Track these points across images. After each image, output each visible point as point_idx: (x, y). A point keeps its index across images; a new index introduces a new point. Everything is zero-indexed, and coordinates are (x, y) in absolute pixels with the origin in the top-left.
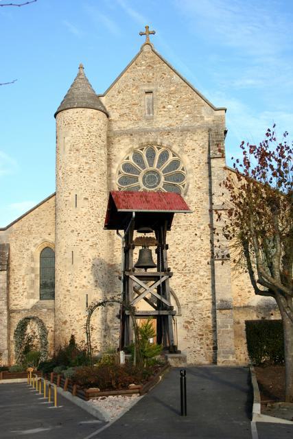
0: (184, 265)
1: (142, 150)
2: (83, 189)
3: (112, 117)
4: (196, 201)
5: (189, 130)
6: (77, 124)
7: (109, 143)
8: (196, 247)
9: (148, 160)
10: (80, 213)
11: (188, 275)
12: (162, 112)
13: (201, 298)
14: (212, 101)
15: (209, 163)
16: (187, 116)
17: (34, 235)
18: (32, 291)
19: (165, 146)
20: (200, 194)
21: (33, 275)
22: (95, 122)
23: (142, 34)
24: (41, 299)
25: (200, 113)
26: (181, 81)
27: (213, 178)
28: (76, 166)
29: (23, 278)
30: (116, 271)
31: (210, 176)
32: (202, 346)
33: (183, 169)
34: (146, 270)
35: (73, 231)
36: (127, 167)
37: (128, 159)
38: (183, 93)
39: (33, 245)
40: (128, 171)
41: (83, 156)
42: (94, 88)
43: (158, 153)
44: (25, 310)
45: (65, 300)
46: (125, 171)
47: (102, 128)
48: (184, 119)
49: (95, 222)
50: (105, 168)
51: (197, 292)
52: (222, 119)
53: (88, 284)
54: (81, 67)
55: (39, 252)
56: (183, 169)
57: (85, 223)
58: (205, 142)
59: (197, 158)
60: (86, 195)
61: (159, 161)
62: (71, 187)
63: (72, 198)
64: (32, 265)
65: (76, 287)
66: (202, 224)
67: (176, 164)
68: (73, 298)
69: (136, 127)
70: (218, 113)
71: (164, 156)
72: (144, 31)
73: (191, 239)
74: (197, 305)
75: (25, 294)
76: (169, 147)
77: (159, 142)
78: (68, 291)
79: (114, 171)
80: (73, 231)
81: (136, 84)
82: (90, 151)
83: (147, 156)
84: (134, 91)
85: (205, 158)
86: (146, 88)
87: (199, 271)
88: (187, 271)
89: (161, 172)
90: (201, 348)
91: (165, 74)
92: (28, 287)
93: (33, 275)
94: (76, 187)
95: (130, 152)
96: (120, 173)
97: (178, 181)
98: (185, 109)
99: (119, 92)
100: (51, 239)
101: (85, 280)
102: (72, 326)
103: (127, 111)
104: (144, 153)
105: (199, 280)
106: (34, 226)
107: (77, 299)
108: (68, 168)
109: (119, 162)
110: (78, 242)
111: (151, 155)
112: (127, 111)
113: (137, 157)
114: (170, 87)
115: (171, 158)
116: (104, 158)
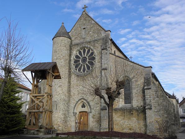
5: (96, 40)
7: (71, 49)
14: (105, 28)
33: (95, 55)
36: (77, 57)
37: (77, 54)
40: (77, 58)
41: (58, 54)
50: (67, 57)
52: (109, 35)
54: (63, 23)
61: (84, 54)
67: (92, 53)
70: (107, 32)
71: (89, 51)
72: (84, 7)
74: (97, 108)
76: (90, 48)
77: (86, 46)
79: (72, 58)
86: (83, 27)
97: (93, 60)
111: (84, 52)
113: (80, 53)
115: (91, 51)
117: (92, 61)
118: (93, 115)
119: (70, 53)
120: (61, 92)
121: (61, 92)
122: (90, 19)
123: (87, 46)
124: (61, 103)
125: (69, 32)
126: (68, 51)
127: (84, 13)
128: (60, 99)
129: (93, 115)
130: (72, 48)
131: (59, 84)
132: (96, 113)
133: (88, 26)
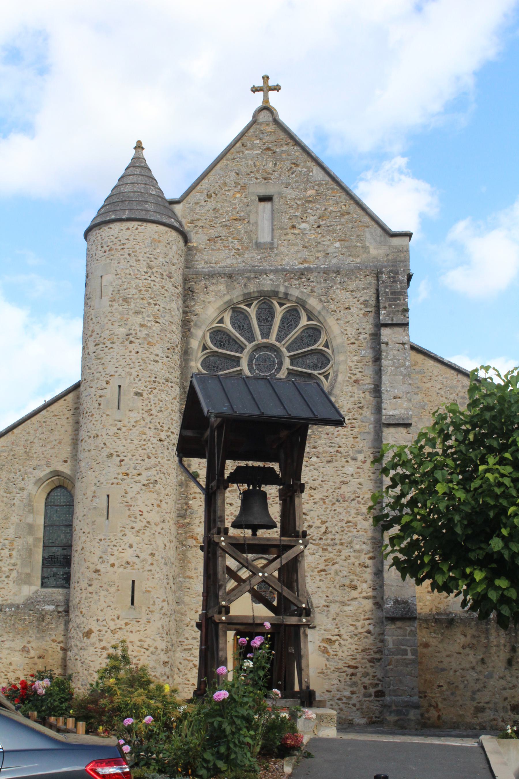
0: (323, 529)
1: (249, 306)
2: (135, 374)
3: (193, 244)
4: (350, 406)
5: (338, 272)
6: (126, 251)
8: (347, 495)
9: (259, 325)
10: (126, 422)
11: (330, 549)
12: (290, 237)
13: (354, 594)
15: (376, 336)
16: (337, 244)
17: (34, 463)
18: (28, 570)
19: (294, 299)
20: (358, 395)
21: (30, 540)
22: (161, 249)
23: (255, 90)
24: (44, 585)
25: (361, 241)
26: (327, 178)
27: (384, 362)
28: (123, 331)
29: (11, 543)
30: (192, 537)
31: (377, 359)
32: (355, 689)
33: (326, 346)
34: (254, 534)
35: (110, 456)
37: (221, 321)
38: (331, 202)
39: (33, 480)
40: (221, 346)
41: (137, 313)
42: (161, 185)
43: (279, 312)
44: (10, 606)
45: (90, 589)
46: (215, 345)
47: (175, 261)
48: (330, 250)
49: (155, 441)
50: (177, 338)
51: (347, 582)
52: (406, 251)
53: (136, 560)
54: (139, 147)
55: (44, 496)
56: (326, 346)
57: (136, 442)
58: (369, 295)
59: (356, 326)
60: (140, 386)
62: (111, 370)
63: (111, 392)
64: (30, 519)
65: (113, 565)
66: (360, 452)
68: (105, 586)
69: (237, 263)
70: (396, 241)
72: (260, 83)
73: (338, 480)
74: (346, 608)
75: (14, 574)
76: (302, 303)
77: (282, 289)
78: (97, 571)
79: (195, 344)
80: (110, 456)
81: (242, 182)
82: (150, 304)
83: (258, 319)
84: (238, 195)
85: (368, 328)
86: (263, 191)
87: (351, 542)
88: (329, 541)
89: (284, 350)
90: (353, 693)
91: (297, 165)
92: (19, 562)
93: (30, 540)
94: (120, 370)
95: (225, 311)
96: (205, 348)
97: (315, 367)
98: (334, 232)
99: (209, 196)
100: (66, 469)
101: (130, 551)
102: (101, 640)
103: (224, 232)
104: (252, 311)
105: (352, 560)
106: (37, 445)
107: (113, 589)
108: (106, 334)
109: (204, 328)
110: (120, 476)
112: (224, 232)
114: (306, 190)
115: (304, 321)
116: (177, 316)
117: (315, 373)
118: (323, 640)
119: (185, 312)
120: (158, 519)
121: (158, 519)
122: (297, 152)
123: (286, 294)
124: (157, 576)
125: (178, 202)
126: (180, 302)
127: (264, 116)
128: (152, 555)
129: (323, 640)
130: (198, 287)
131: (145, 474)
132: (342, 632)
133: (287, 192)
